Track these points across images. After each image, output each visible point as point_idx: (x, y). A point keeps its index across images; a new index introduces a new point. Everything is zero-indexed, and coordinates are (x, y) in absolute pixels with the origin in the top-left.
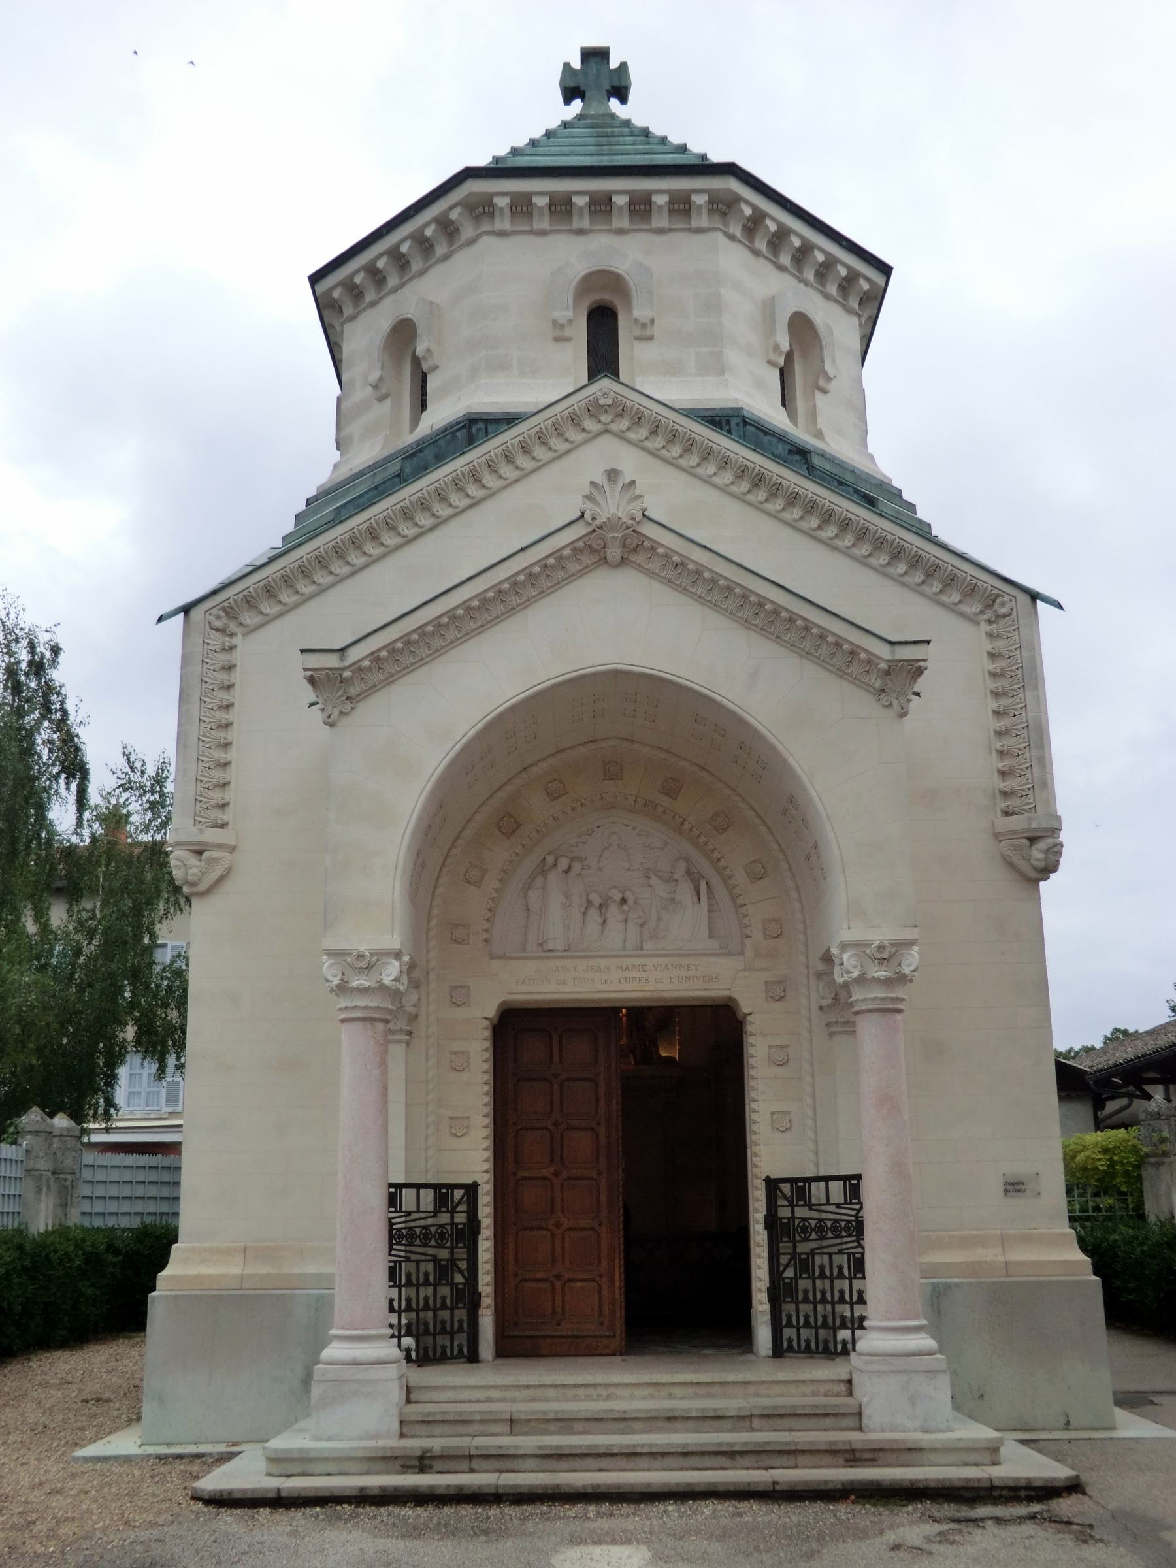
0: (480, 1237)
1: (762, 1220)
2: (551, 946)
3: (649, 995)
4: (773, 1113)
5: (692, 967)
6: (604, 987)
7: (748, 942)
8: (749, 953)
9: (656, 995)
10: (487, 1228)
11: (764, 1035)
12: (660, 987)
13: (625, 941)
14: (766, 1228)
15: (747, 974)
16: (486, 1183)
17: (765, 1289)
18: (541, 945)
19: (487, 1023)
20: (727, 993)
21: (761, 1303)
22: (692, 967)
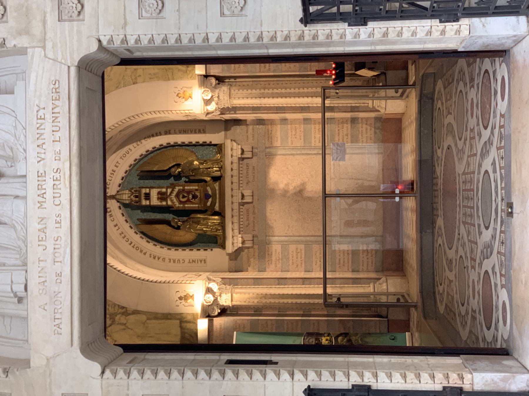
0: (375, 387)
1: (355, 29)
2: (19, 288)
3: (75, 169)
4: (222, 14)
5: (41, 113)
6: (66, 224)
7: (10, 43)
8: (23, 42)
9: (75, 160)
10: (362, 376)
11: (125, 24)
12: (65, 154)
13: (17, 197)
14: (365, 24)
15: (49, 45)
16: (306, 375)
17: (441, 26)
18: (20, 300)
19: (108, 372)
20: (73, 70)
21: (458, 32)
22: (41, 113)
